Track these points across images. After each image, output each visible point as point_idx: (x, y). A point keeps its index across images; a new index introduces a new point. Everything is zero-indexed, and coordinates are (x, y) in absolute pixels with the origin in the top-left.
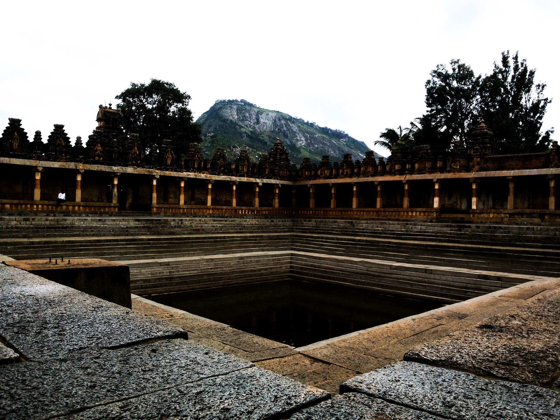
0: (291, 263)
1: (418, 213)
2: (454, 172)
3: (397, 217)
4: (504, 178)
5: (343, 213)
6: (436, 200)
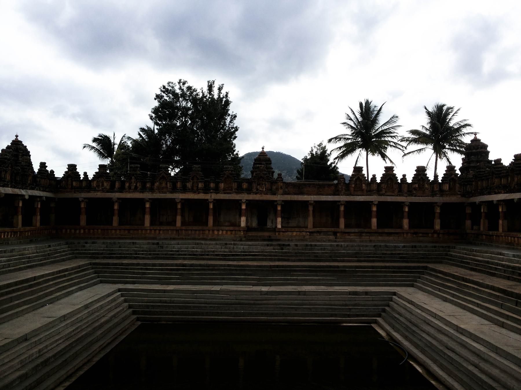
0: (125, 301)
1: (224, 232)
2: (261, 194)
3: (201, 236)
4: (306, 203)
5: (131, 232)
6: (243, 219)
